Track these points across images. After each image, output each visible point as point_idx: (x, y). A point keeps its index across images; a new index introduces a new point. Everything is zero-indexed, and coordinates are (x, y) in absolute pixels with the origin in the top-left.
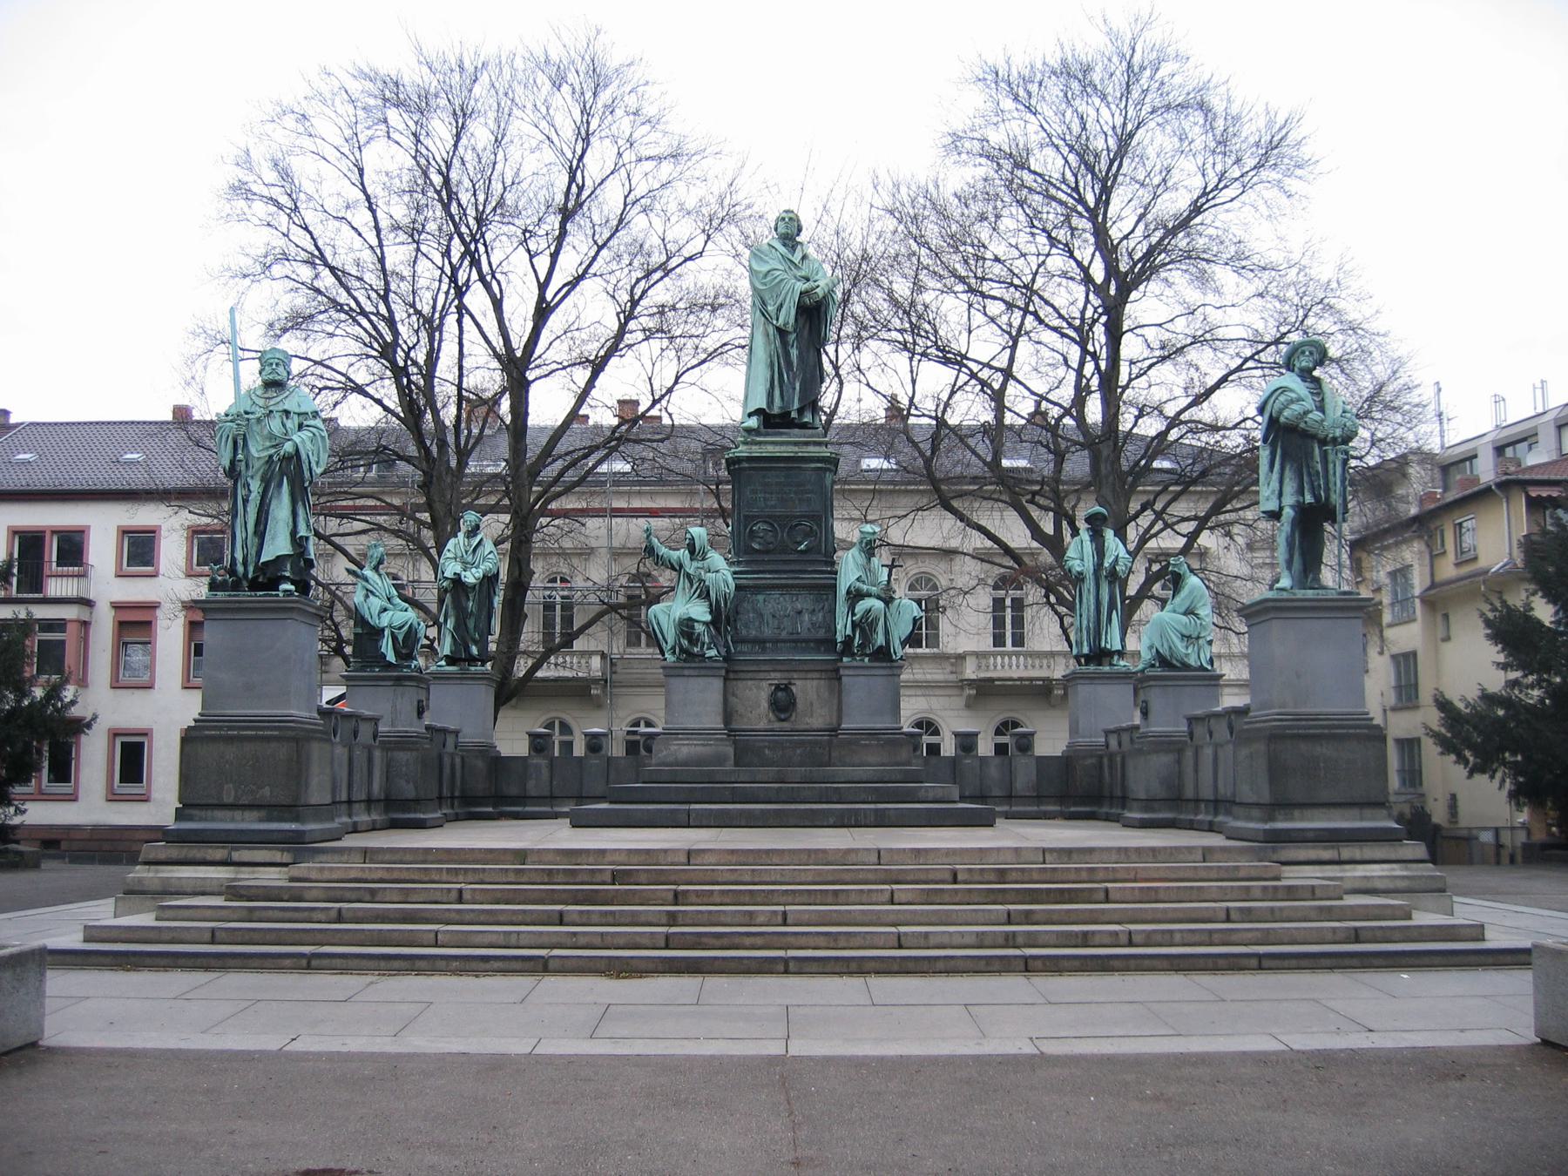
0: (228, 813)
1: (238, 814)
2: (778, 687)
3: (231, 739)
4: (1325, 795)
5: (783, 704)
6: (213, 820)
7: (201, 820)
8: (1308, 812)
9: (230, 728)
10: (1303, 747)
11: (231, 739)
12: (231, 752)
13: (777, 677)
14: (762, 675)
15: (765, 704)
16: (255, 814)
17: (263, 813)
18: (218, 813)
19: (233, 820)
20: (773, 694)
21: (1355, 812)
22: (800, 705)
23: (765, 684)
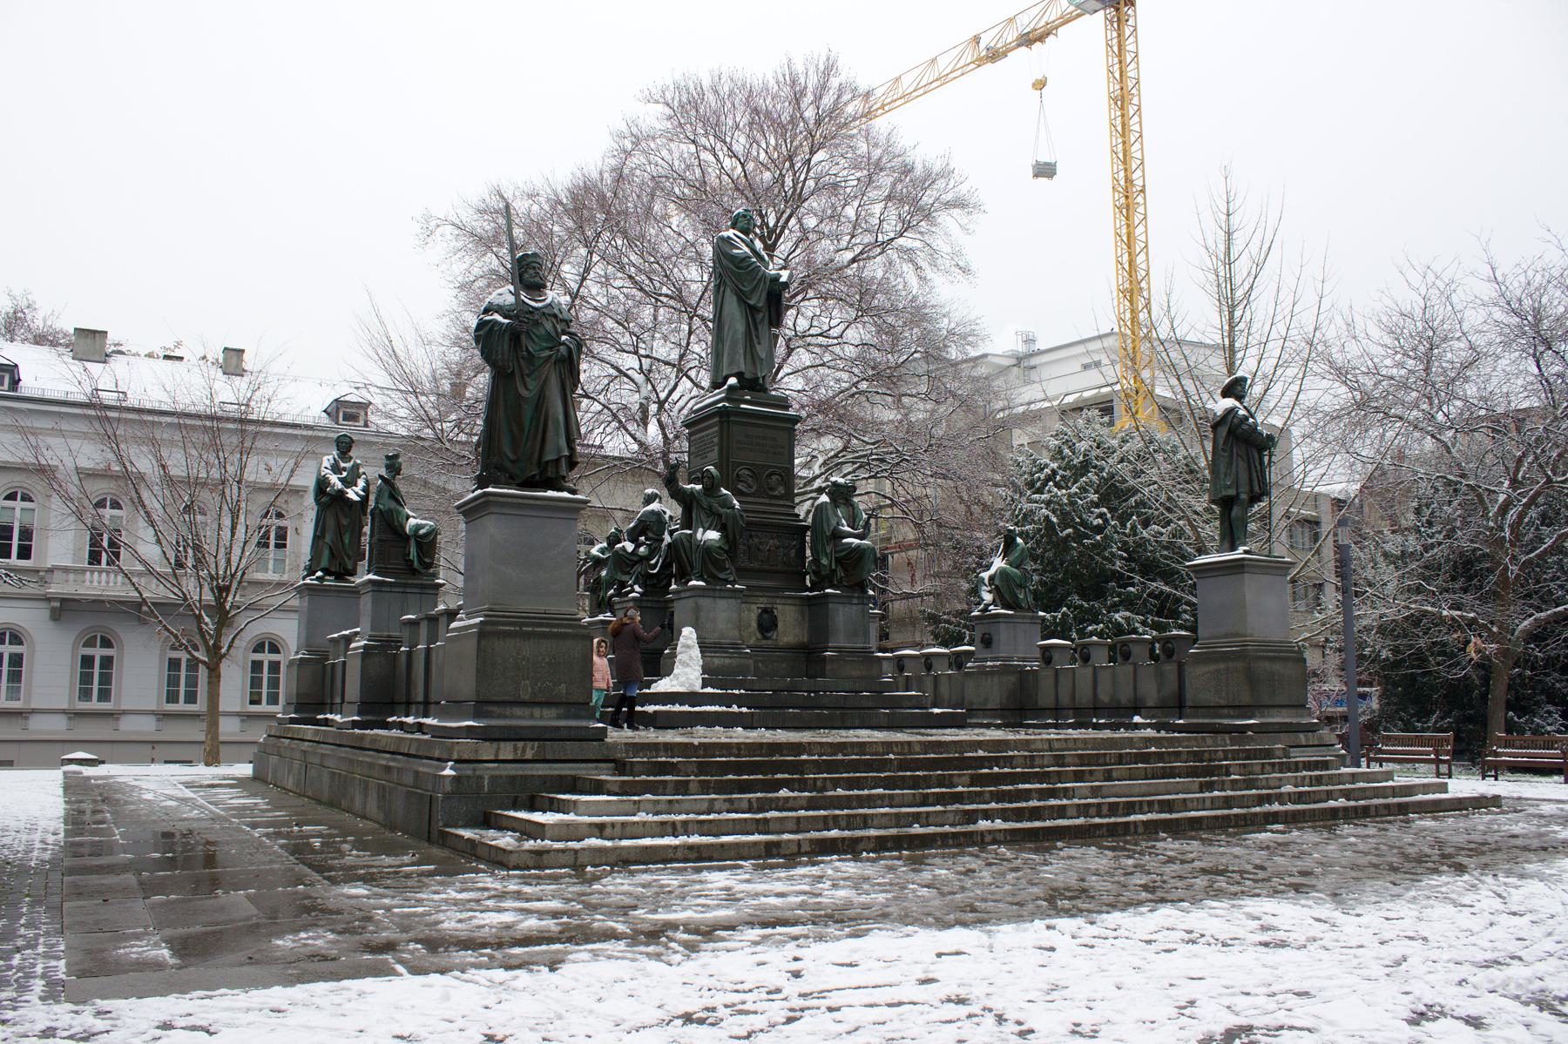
0: (526, 711)
1: (537, 712)
2: (765, 610)
3: (528, 636)
4: (1279, 700)
5: (767, 623)
6: (512, 717)
7: (500, 716)
8: (1273, 711)
9: (542, 625)
10: (1267, 665)
11: (528, 636)
12: (528, 649)
13: (763, 602)
14: (752, 600)
15: (754, 624)
16: (553, 712)
17: (561, 711)
18: (518, 711)
19: (532, 717)
20: (760, 616)
21: (1294, 711)
22: (780, 625)
23: (754, 607)
